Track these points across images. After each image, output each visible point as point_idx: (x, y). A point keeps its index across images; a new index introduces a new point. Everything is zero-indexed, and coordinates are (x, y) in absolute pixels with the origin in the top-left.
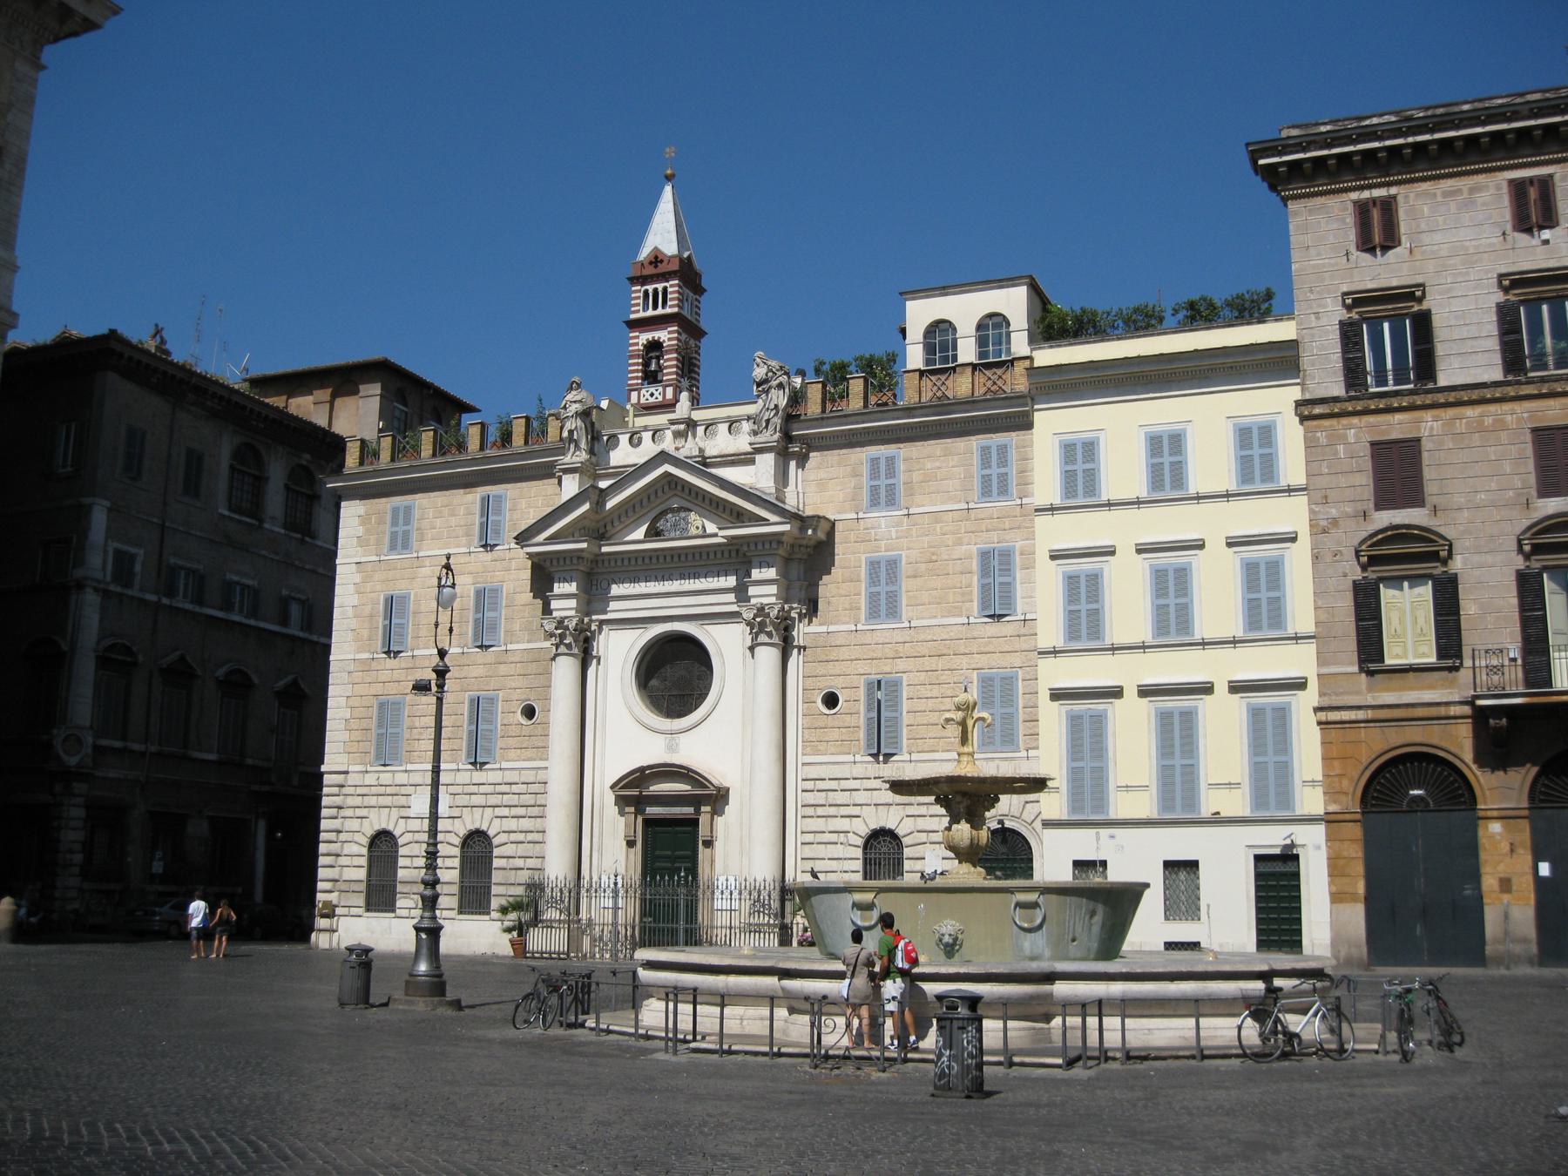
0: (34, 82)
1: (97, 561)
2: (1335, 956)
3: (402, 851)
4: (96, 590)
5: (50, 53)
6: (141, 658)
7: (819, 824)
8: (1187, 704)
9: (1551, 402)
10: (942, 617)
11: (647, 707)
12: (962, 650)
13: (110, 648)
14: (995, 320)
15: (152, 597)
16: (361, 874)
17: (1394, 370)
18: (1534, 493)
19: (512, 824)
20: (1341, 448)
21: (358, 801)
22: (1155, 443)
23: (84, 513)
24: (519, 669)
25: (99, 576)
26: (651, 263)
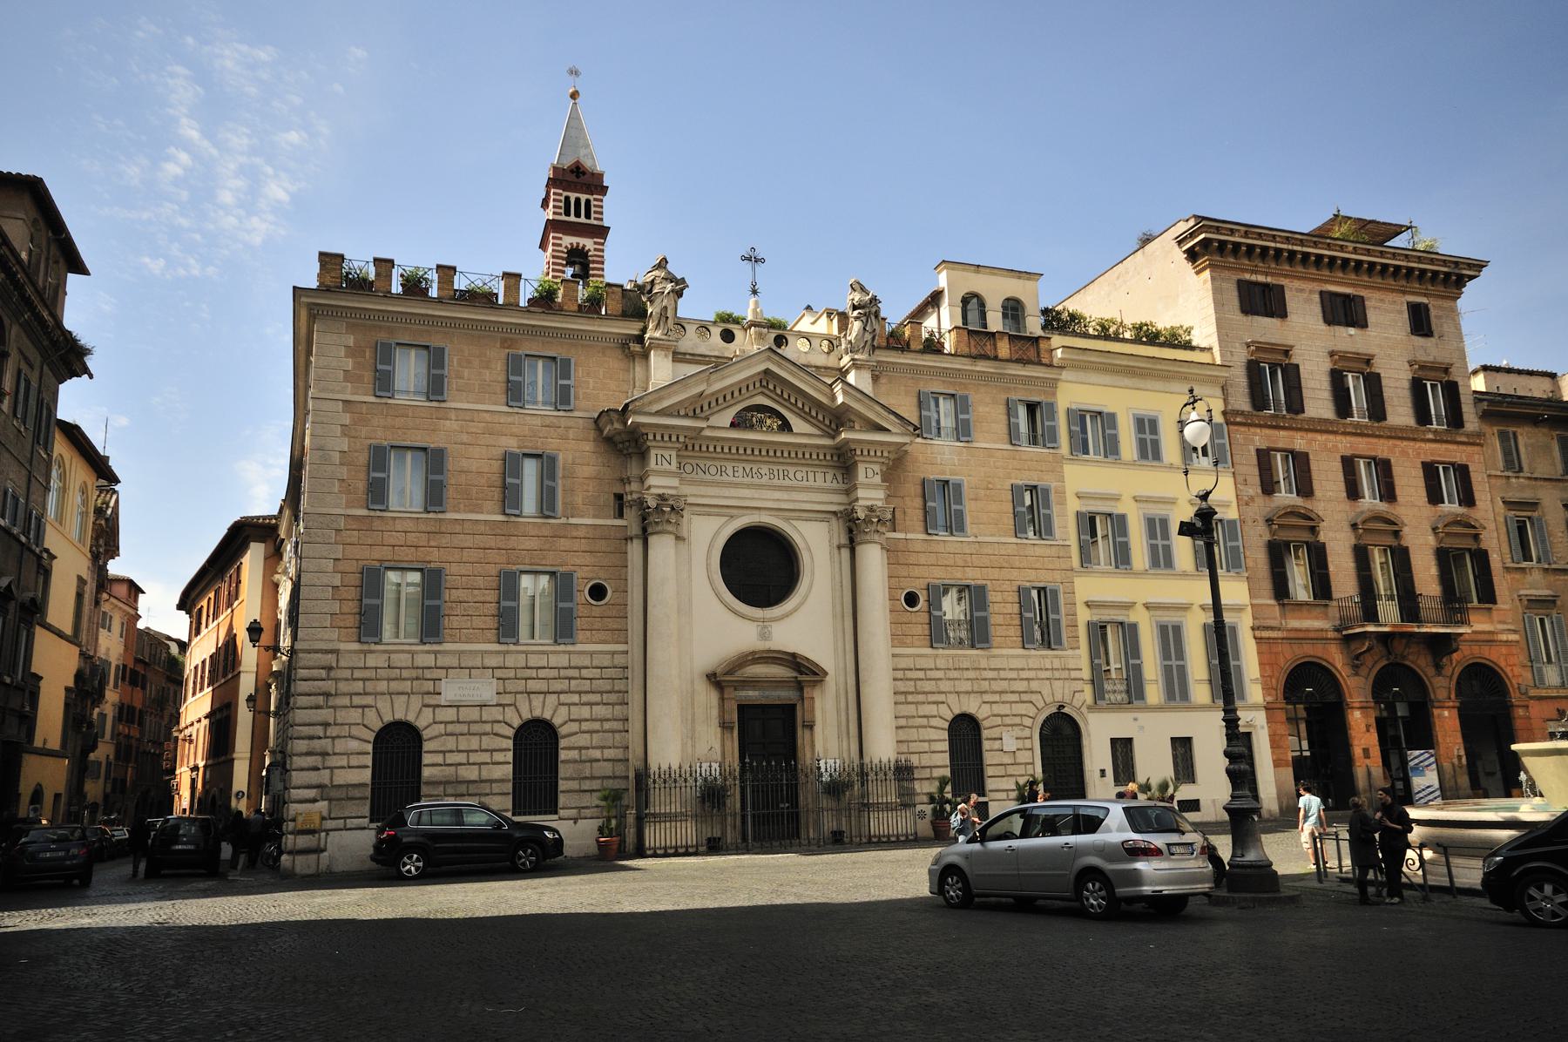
2: (1281, 809)
7: (911, 710)
8: (1175, 619)
9: (1360, 439)
10: (1000, 536)
12: (1017, 565)
16: (508, 770)
24: (584, 545)
26: (572, 171)
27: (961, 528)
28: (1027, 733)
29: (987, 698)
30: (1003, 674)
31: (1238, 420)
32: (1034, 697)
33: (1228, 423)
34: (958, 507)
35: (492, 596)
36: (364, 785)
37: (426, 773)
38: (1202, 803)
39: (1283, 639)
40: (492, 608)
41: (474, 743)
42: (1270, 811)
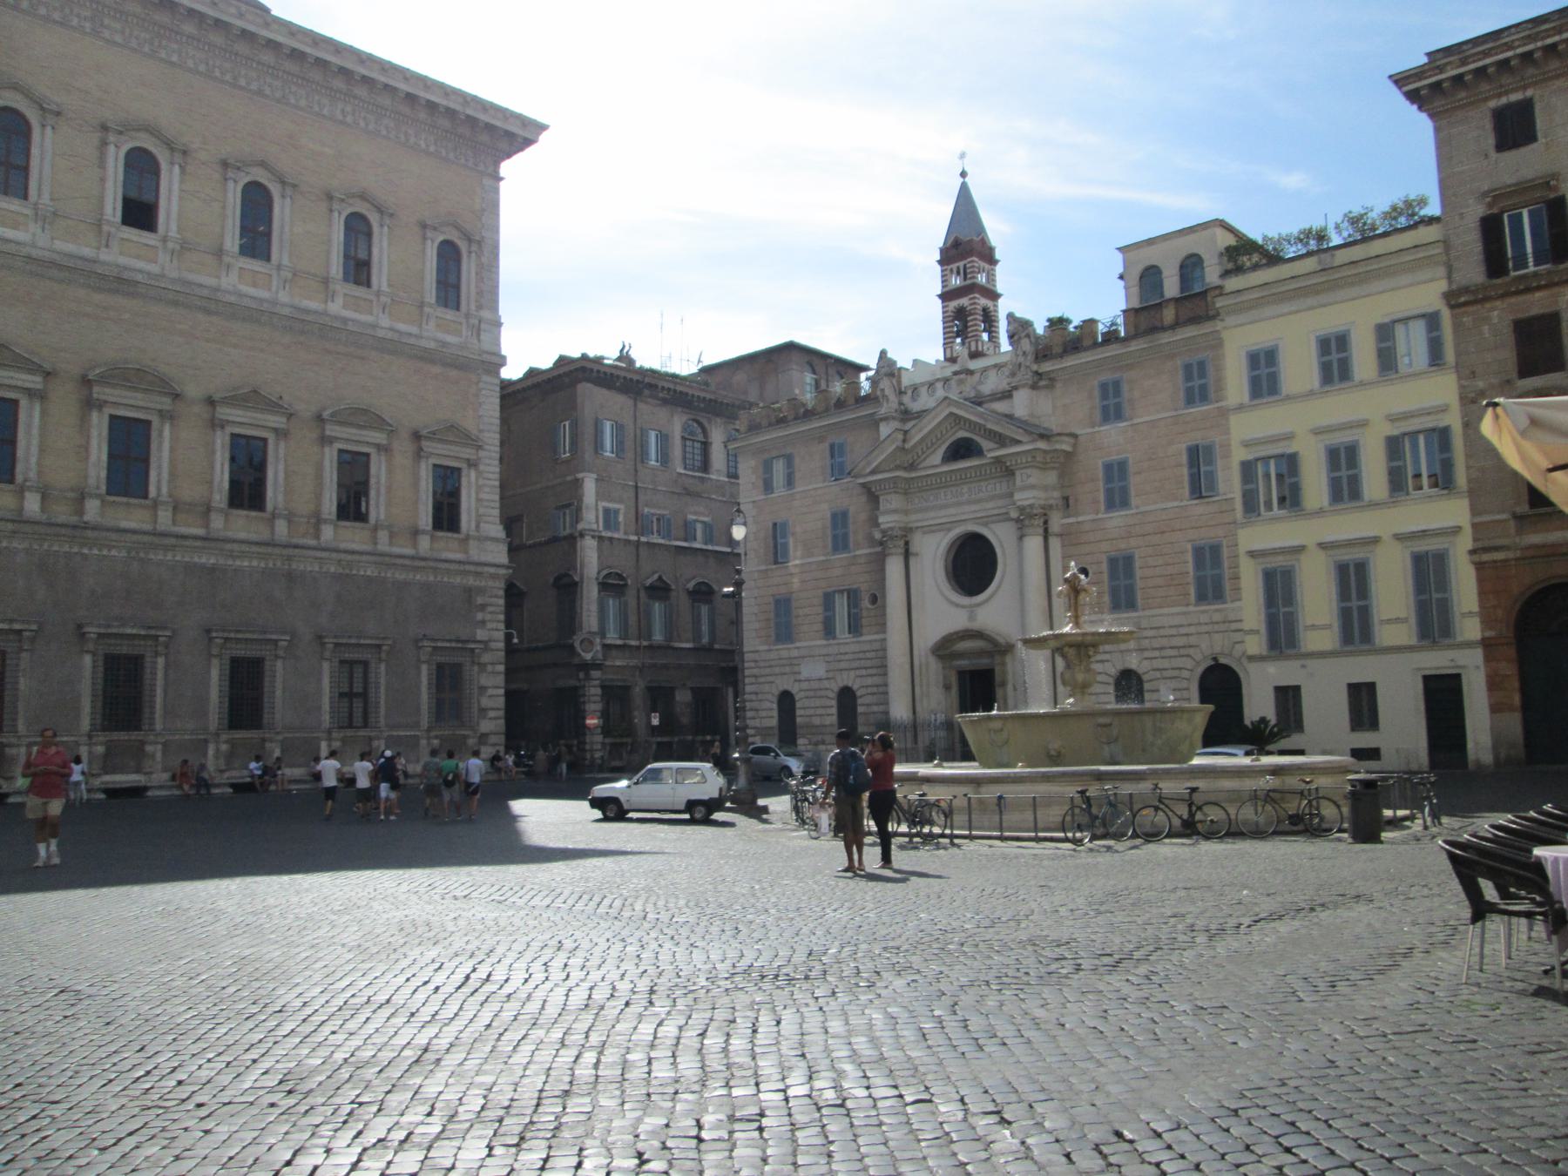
0: (497, 191)
1: (591, 518)
2: (1496, 757)
3: (798, 705)
4: (593, 537)
5: (507, 168)
6: (629, 582)
8: (1357, 556)
11: (954, 589)
13: (605, 577)
14: (1193, 260)
15: (634, 538)
17: (1535, 252)
18: (1515, 375)
19: (869, 681)
20: (1486, 328)
21: (768, 671)
22: (1324, 345)
23: (577, 484)
25: (594, 527)
27: (1125, 503)
28: (1184, 684)
29: (1147, 654)
30: (1162, 632)
31: (1463, 299)
32: (1191, 651)
33: (1452, 307)
34: (1208, 468)
35: (820, 610)
36: (772, 728)
37: (798, 720)
38: (1382, 752)
39: (1517, 559)
40: (820, 618)
41: (818, 702)
42: (1478, 762)
